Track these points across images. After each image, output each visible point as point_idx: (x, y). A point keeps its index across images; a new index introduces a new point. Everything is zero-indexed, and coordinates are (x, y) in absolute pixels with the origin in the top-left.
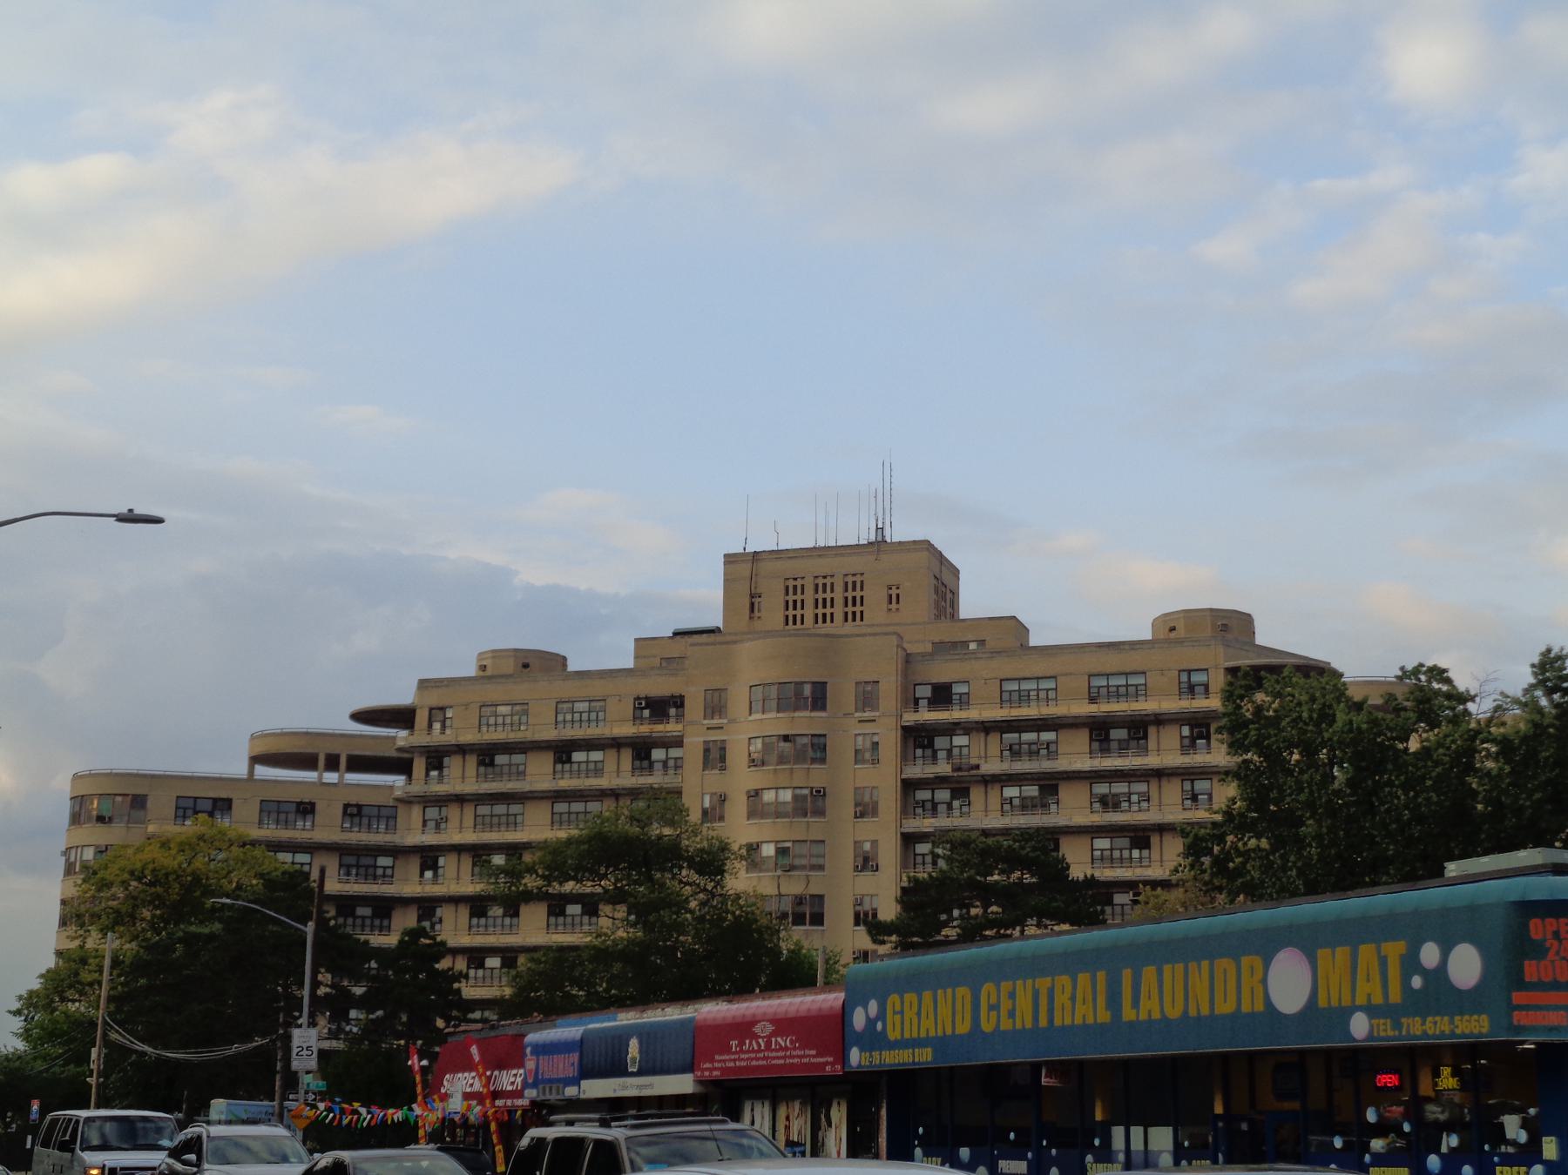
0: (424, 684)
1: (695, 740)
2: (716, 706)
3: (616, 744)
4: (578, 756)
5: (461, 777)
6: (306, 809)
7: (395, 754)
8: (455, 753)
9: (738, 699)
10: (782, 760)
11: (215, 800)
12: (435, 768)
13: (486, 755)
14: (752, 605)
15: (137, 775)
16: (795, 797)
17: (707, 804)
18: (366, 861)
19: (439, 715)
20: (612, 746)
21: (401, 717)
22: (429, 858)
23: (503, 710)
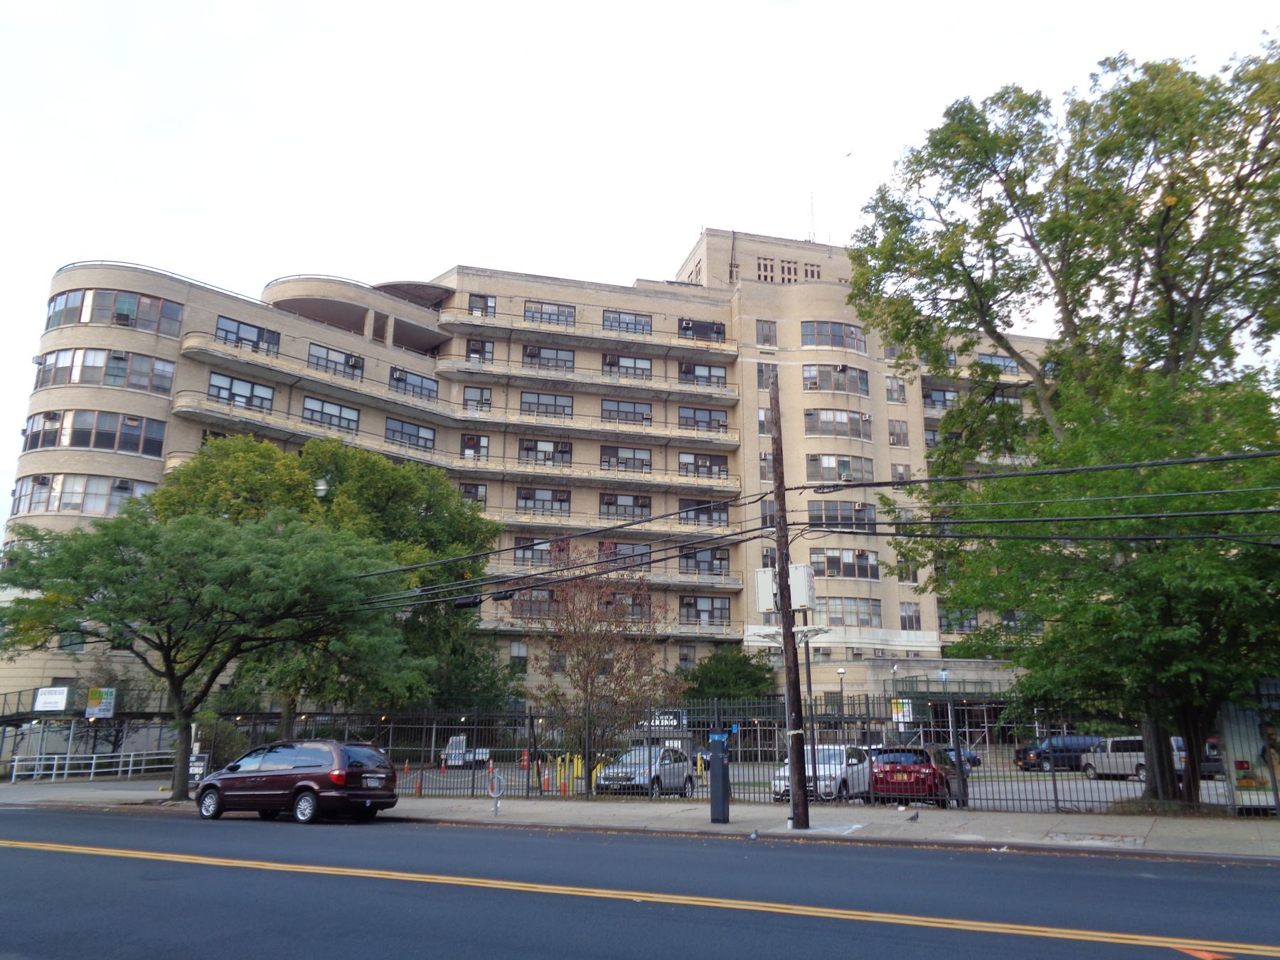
0: (463, 271)
1: (749, 362)
2: (767, 333)
3: (666, 354)
4: (625, 362)
5: (505, 362)
6: (355, 364)
7: (437, 330)
8: (501, 340)
9: (789, 331)
10: (838, 387)
11: (261, 330)
12: (475, 351)
13: (533, 346)
14: (731, 272)
15: (171, 278)
16: (850, 419)
17: (762, 418)
18: (409, 429)
19: (480, 303)
20: (658, 357)
21: (436, 297)
22: (471, 435)
23: (547, 308)
